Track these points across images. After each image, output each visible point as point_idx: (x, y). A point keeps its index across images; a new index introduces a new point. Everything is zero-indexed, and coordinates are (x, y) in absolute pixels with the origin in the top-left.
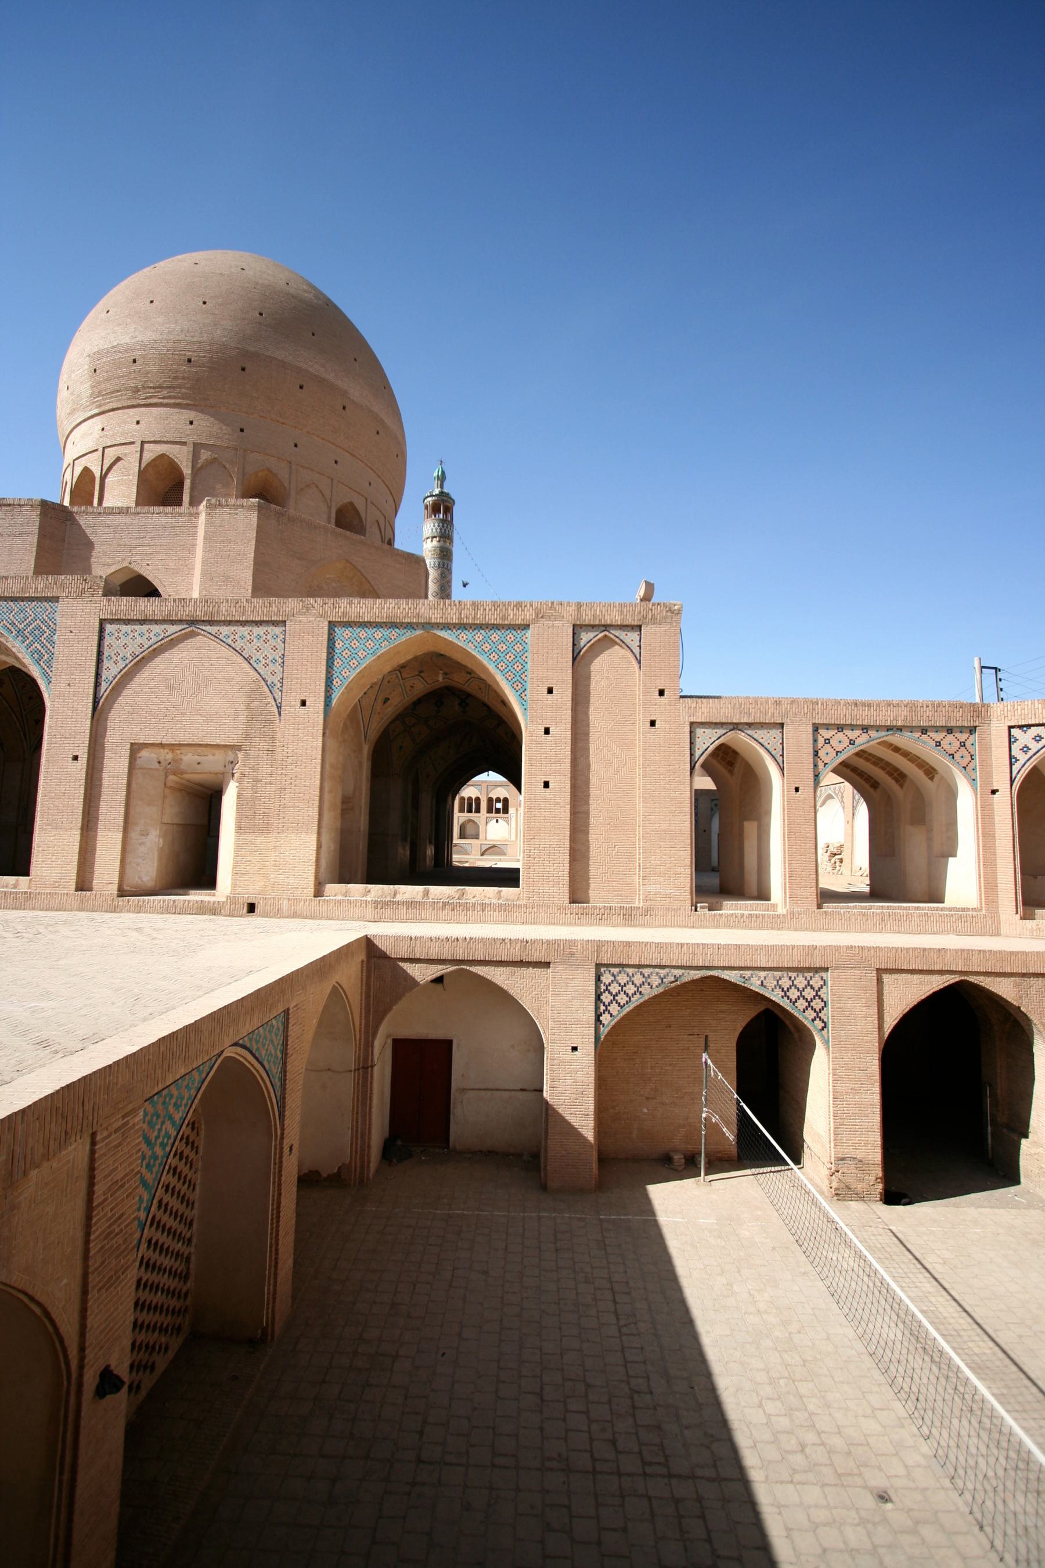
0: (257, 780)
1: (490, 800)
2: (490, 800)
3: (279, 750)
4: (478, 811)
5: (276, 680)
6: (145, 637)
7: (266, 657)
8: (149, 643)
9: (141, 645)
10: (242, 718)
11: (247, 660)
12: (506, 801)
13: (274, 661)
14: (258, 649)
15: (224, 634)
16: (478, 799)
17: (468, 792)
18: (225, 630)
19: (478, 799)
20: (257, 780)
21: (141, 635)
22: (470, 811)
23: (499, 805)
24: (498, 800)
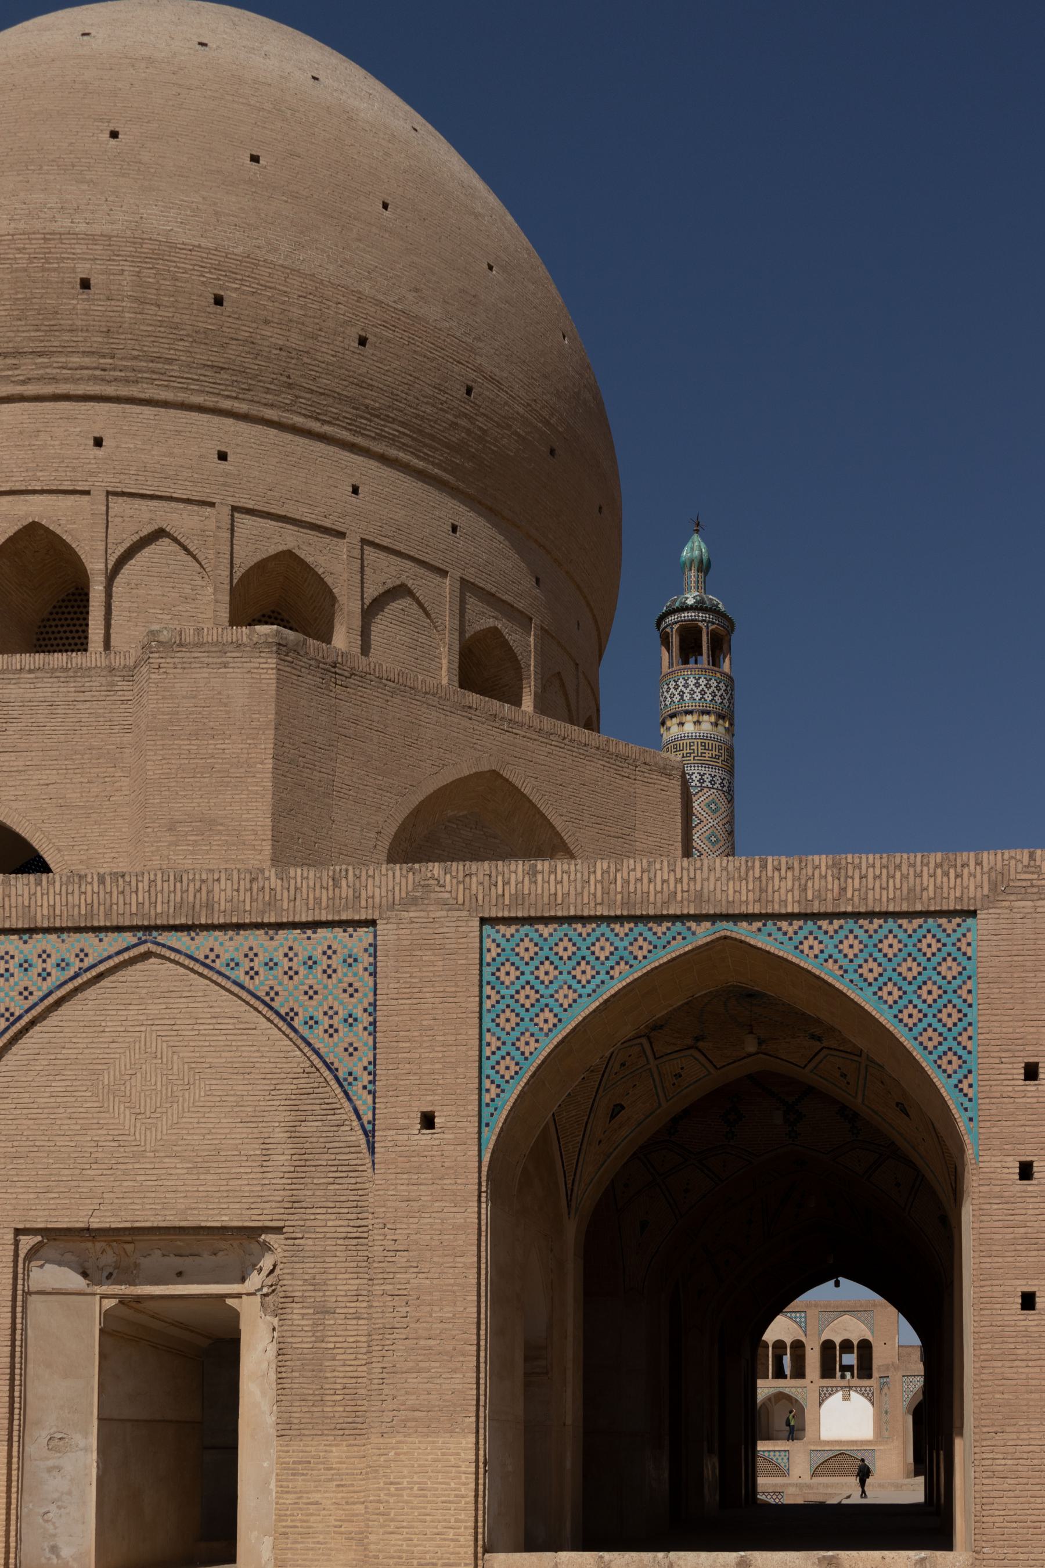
0: (324, 1311)
1: (827, 1347)
2: (827, 1347)
3: (376, 1235)
4: (799, 1372)
5: (357, 1065)
6: (34, 972)
7: (330, 1013)
8: (46, 987)
9: (26, 992)
10: (282, 1159)
11: (287, 1018)
12: (865, 1348)
13: (351, 1020)
14: (311, 993)
15: (225, 957)
16: (798, 1347)
17: (780, 1329)
18: (228, 947)
19: (798, 1347)
20: (324, 1311)
21: (25, 966)
22: (779, 1374)
23: (850, 1359)
24: (847, 1346)
